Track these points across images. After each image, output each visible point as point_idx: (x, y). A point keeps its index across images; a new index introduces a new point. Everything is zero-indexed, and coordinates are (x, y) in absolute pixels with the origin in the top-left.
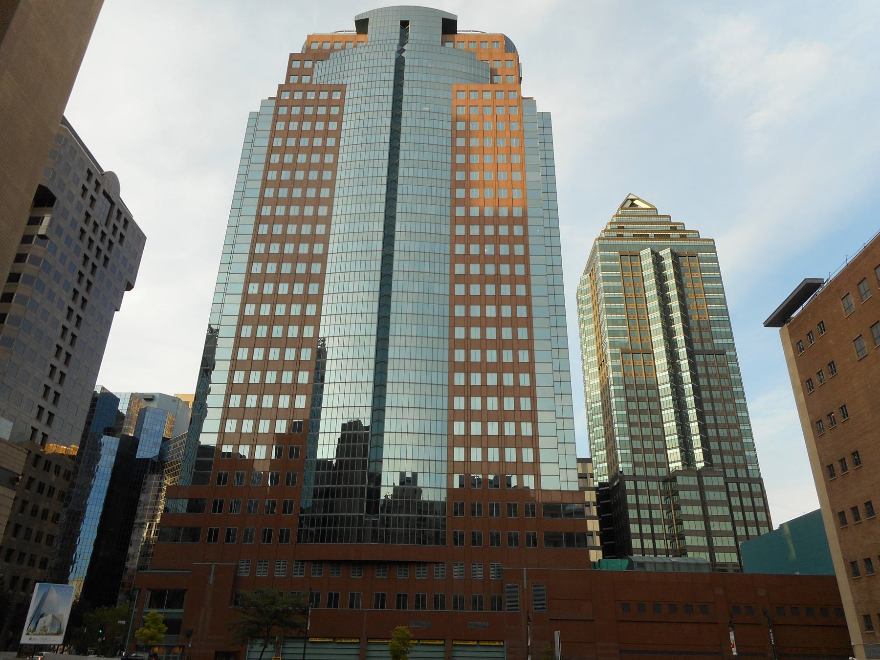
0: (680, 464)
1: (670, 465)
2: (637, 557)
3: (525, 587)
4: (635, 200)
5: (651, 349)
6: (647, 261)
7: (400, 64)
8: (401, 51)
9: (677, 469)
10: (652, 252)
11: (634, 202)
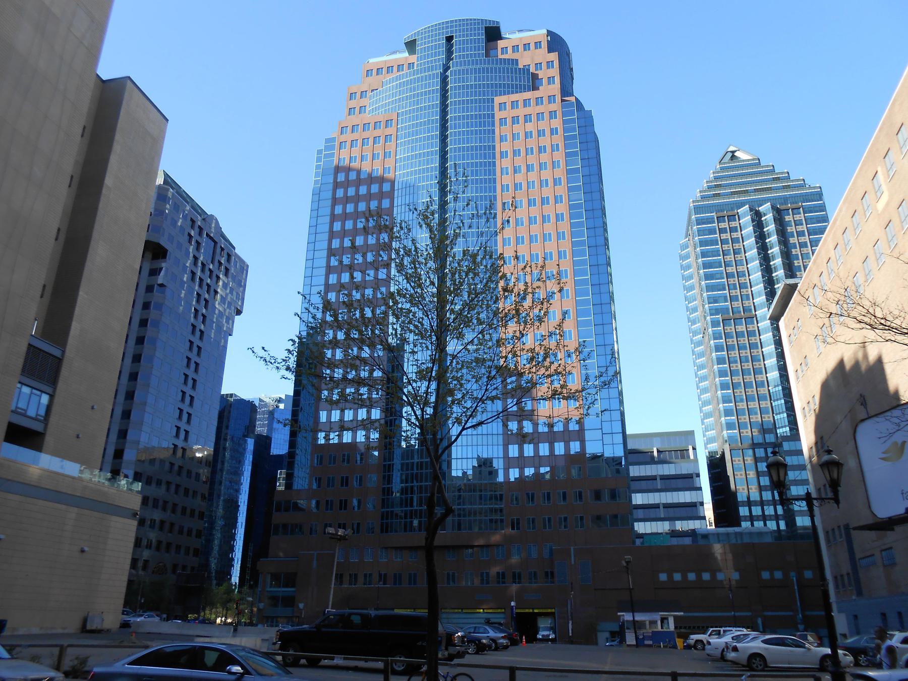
0: (788, 429)
1: (778, 430)
2: (745, 525)
3: (573, 563)
4: (736, 151)
5: (754, 313)
6: (746, 219)
7: (444, 81)
8: (446, 68)
9: (785, 435)
10: (751, 210)
11: (736, 154)
